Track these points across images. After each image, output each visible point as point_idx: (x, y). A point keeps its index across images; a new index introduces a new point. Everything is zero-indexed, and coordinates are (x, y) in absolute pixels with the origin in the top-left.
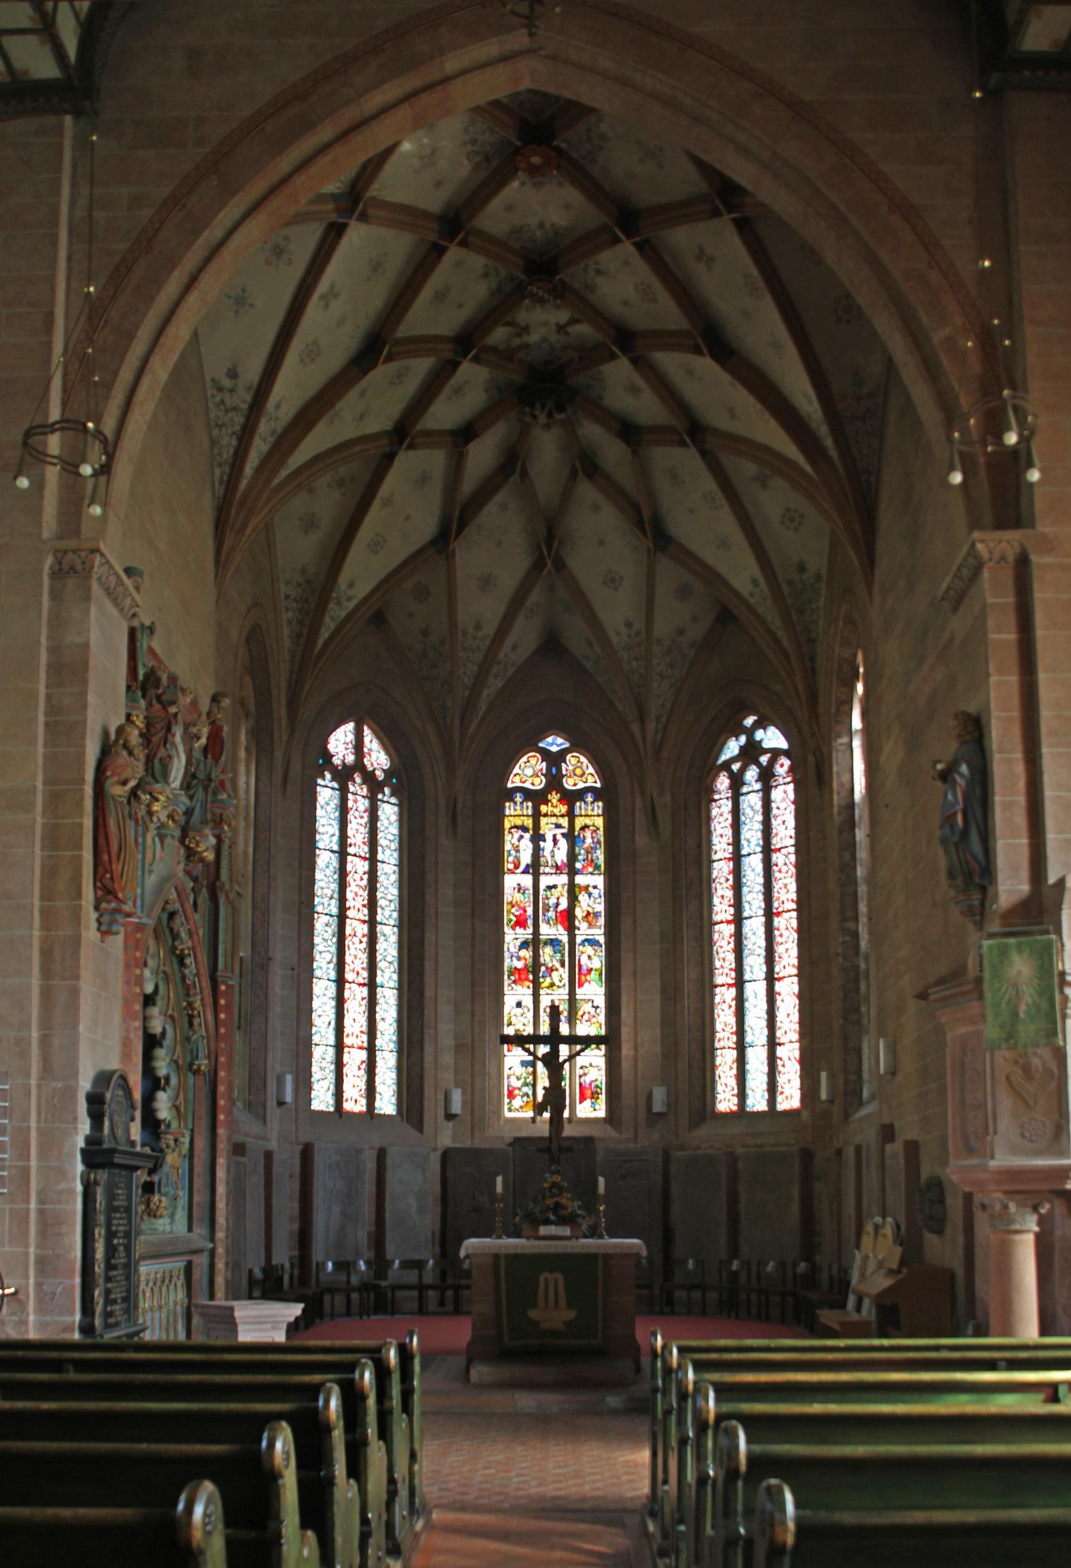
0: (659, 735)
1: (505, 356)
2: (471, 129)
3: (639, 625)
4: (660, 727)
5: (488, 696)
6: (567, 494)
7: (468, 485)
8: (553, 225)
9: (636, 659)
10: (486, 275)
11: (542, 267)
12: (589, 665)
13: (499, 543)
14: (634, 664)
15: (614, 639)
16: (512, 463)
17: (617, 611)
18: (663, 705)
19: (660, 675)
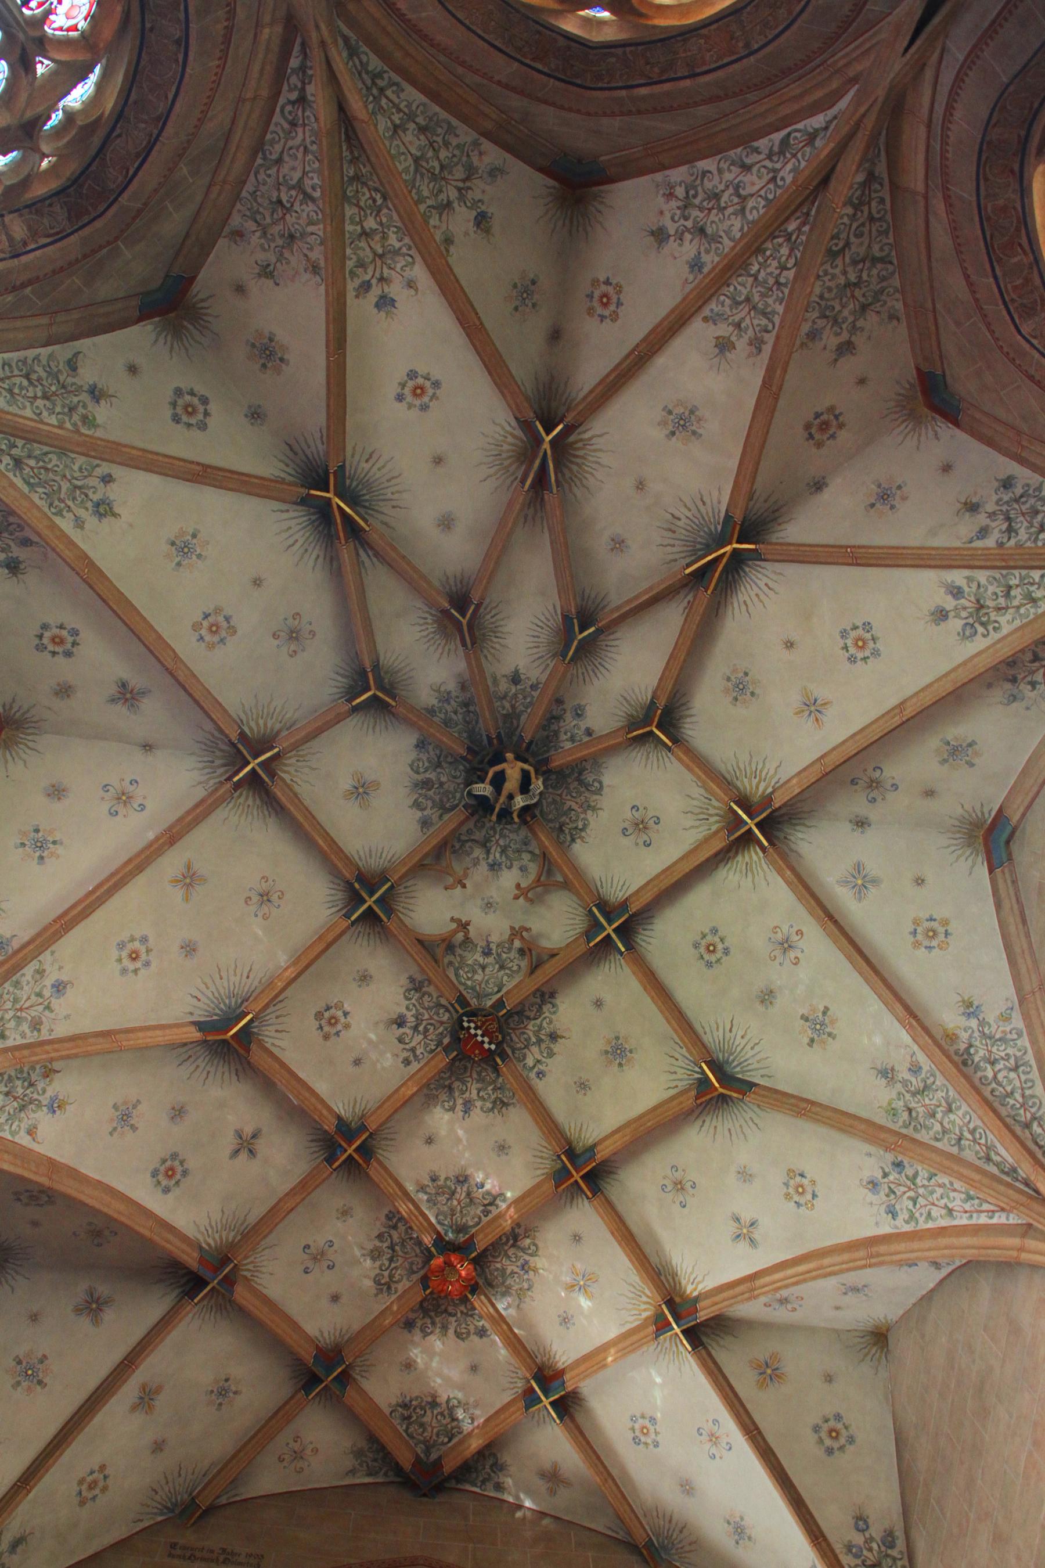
0: (294, 63)
1: (554, 875)
2: (526, 1285)
3: (360, 309)
4: (294, 80)
5: (746, 168)
6: (498, 551)
7: (669, 624)
8: (452, 1109)
9: (365, 234)
10: (554, 1037)
11: (480, 1042)
12: (493, 155)
13: (640, 486)
14: (371, 223)
15: (419, 272)
16: (583, 631)
17: (410, 333)
18: (293, 124)
19: (308, 197)
